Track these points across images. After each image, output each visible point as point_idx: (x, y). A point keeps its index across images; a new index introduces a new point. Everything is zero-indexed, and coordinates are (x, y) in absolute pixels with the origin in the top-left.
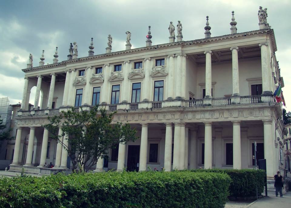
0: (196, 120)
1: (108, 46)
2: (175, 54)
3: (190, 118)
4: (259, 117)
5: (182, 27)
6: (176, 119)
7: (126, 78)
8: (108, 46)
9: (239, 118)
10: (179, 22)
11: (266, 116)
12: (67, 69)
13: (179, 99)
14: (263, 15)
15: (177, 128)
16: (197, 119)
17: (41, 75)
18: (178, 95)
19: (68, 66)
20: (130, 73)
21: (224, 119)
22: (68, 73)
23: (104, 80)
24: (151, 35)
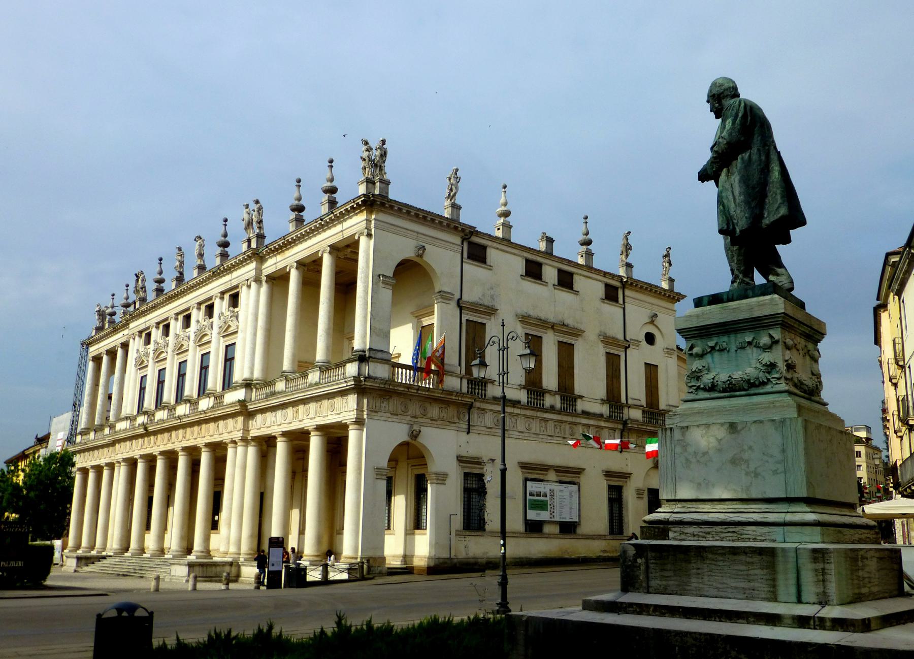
0: (265, 429)
1: (178, 274)
2: (247, 280)
3: (261, 426)
4: (342, 415)
5: (263, 211)
6: (238, 431)
7: (191, 343)
8: (178, 274)
9: (317, 419)
10: (257, 202)
11: (350, 411)
12: (130, 334)
13: (248, 385)
14: (367, 160)
15: (240, 449)
16: (267, 427)
17: (107, 351)
18: (246, 375)
19: (132, 325)
20: (195, 333)
21: (298, 423)
22: (131, 340)
23: (167, 352)
24: (227, 239)
